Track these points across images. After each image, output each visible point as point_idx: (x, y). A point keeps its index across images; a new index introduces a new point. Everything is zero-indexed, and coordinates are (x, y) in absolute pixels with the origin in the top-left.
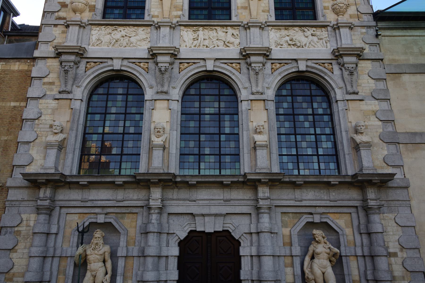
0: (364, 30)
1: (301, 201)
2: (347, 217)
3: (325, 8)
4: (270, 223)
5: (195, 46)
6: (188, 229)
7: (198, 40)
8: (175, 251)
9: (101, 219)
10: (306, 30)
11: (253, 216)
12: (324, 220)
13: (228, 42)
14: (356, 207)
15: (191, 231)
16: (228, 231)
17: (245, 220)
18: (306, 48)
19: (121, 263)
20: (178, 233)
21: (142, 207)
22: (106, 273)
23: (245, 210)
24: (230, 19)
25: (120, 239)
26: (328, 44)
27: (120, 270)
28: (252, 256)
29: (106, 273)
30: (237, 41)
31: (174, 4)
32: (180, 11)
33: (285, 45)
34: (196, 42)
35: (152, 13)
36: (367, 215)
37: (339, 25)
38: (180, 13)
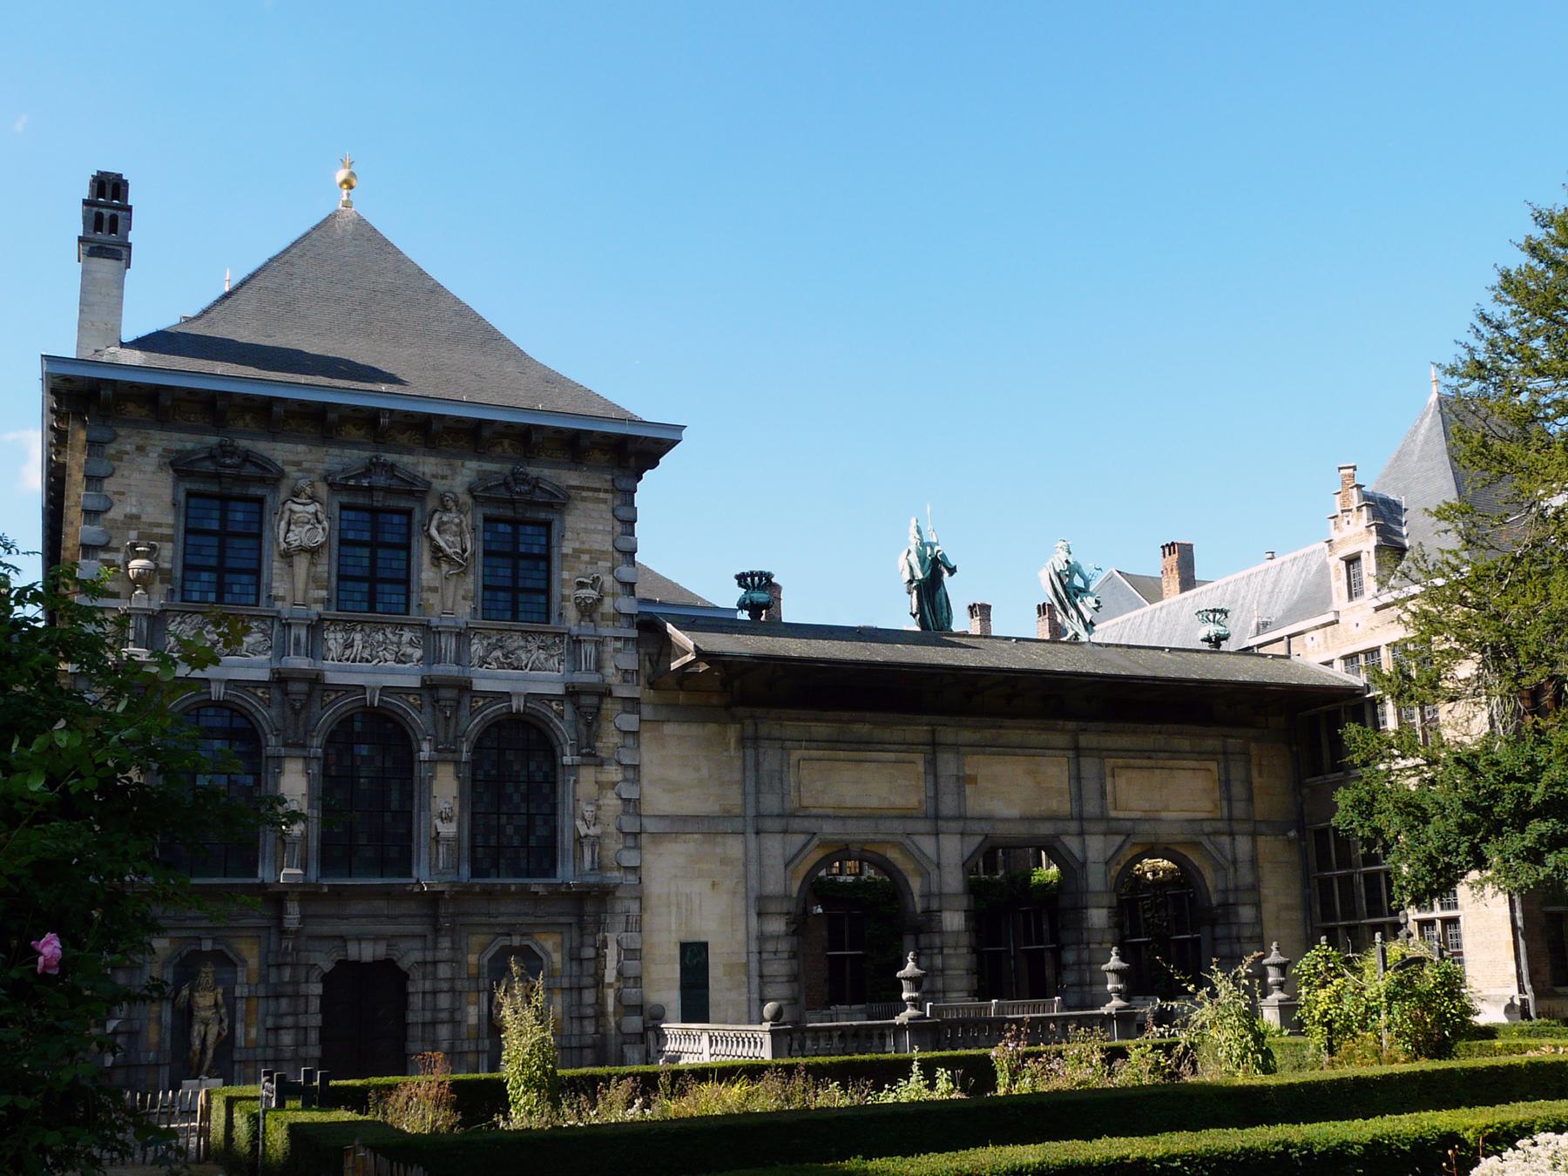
0: (619, 645)
1: (497, 917)
2: (557, 938)
3: (564, 598)
4: (452, 949)
5: (347, 660)
6: (335, 957)
7: (352, 646)
8: (317, 989)
9: (207, 946)
10: (530, 638)
11: (430, 938)
12: (526, 943)
13: (403, 655)
14: (571, 924)
15: (339, 963)
16: (392, 960)
17: (418, 944)
18: (527, 671)
19: (241, 1006)
20: (321, 964)
21: (269, 927)
22: (221, 1021)
23: (418, 929)
25: (236, 972)
26: (561, 667)
27: (239, 1015)
28: (424, 993)
29: (221, 1021)
30: (418, 653)
32: (322, 589)
33: (494, 665)
34: (348, 652)
35: (274, 592)
36: (582, 936)
37: (581, 638)
38: (323, 593)
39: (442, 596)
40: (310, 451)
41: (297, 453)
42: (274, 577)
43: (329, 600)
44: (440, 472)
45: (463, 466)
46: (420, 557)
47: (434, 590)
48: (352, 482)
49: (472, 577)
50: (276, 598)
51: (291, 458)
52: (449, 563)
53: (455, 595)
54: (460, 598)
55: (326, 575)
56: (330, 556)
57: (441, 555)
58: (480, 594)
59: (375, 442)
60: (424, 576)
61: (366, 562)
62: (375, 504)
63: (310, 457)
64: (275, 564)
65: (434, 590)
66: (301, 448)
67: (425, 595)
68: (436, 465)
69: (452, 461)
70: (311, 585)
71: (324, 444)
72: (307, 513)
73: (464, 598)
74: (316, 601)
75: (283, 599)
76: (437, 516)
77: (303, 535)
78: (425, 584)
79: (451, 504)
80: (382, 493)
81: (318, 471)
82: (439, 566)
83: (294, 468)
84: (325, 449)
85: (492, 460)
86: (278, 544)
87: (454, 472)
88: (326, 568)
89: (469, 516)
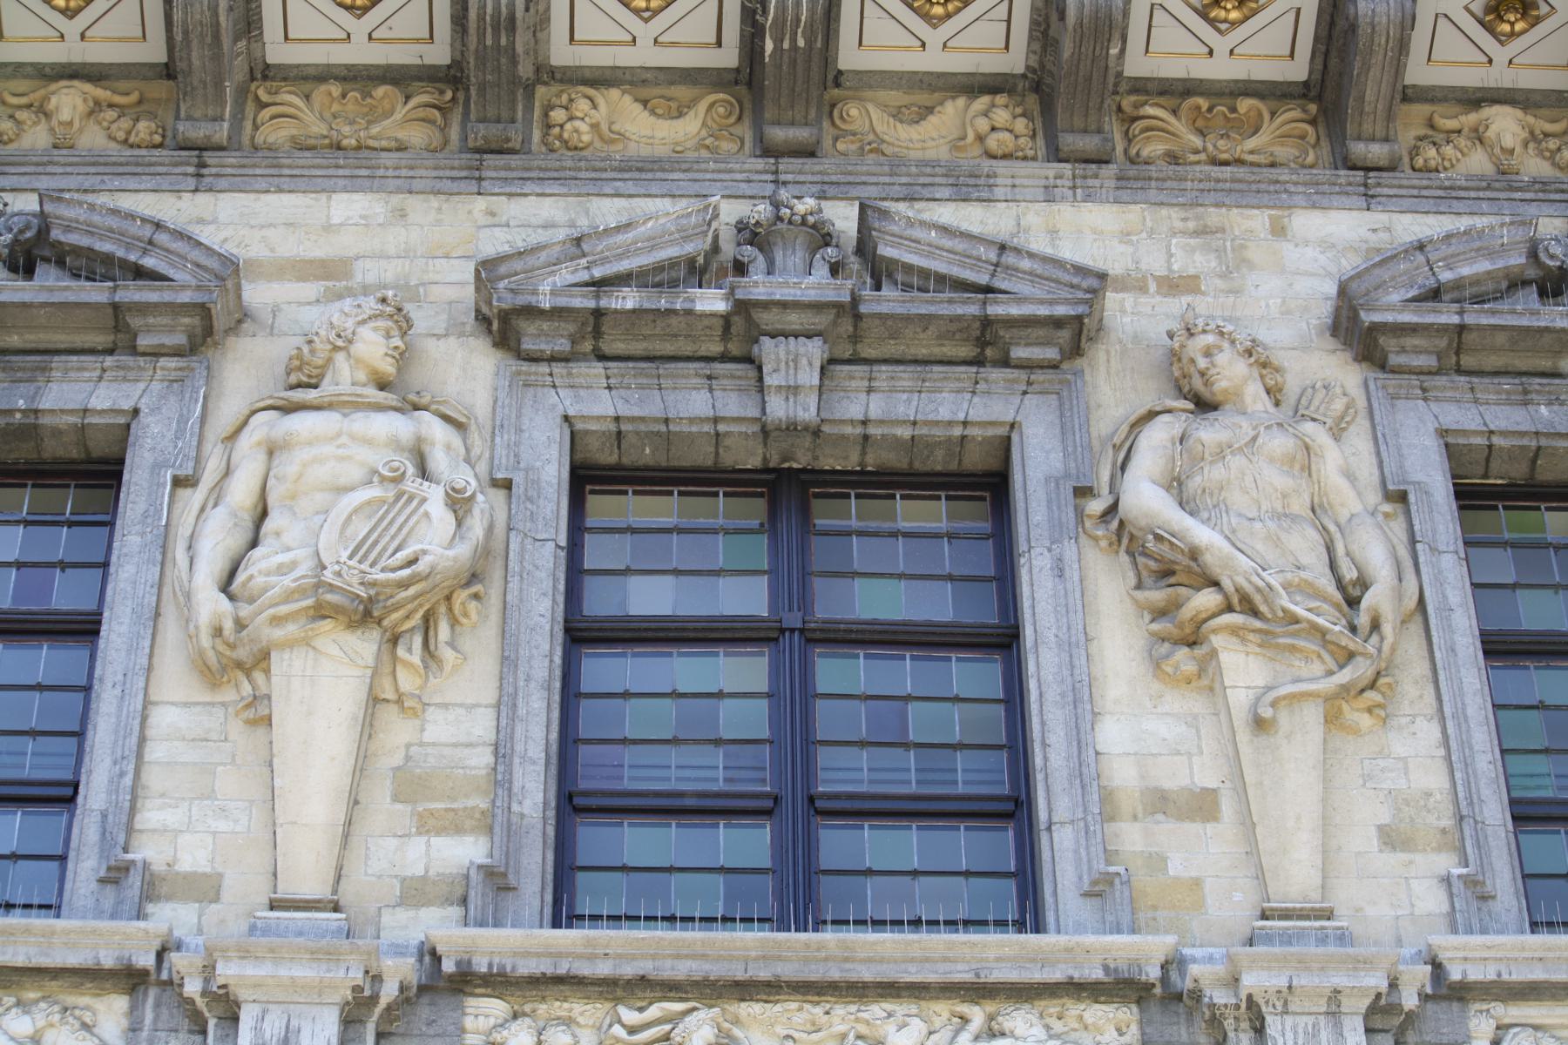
24: (1030, 916)
31: (397, 760)
32: (459, 831)
35: (148, 851)
39: (1248, 825)
40: (401, 214)
41: (328, 228)
42: (154, 778)
43: (497, 880)
44: (1153, 262)
45: (1279, 231)
46: (1079, 644)
47: (1202, 806)
48: (627, 299)
49: (1429, 732)
50: (153, 888)
51: (290, 247)
52: (1267, 640)
53: (1326, 825)
54: (1360, 839)
55: (482, 759)
56: (508, 661)
57: (1206, 600)
58: (1491, 717)
59: (768, 150)
60: (1112, 735)
61: (752, 719)
62: (778, 409)
63: (395, 238)
64: (164, 719)
65: (1202, 806)
66: (348, 207)
67: (1131, 837)
68: (1125, 236)
69: (1214, 216)
70: (382, 807)
71: (477, 181)
72: (368, 442)
73: (1391, 838)
74: (414, 893)
75: (205, 889)
76: (1157, 436)
77: (327, 538)
78: (1123, 775)
79: (1230, 371)
80: (815, 350)
81: (451, 293)
82: (1207, 678)
83: (311, 289)
84: (481, 203)
85: (1449, 196)
86: (187, 620)
87: (1235, 265)
88: (482, 726)
89: (1359, 440)
